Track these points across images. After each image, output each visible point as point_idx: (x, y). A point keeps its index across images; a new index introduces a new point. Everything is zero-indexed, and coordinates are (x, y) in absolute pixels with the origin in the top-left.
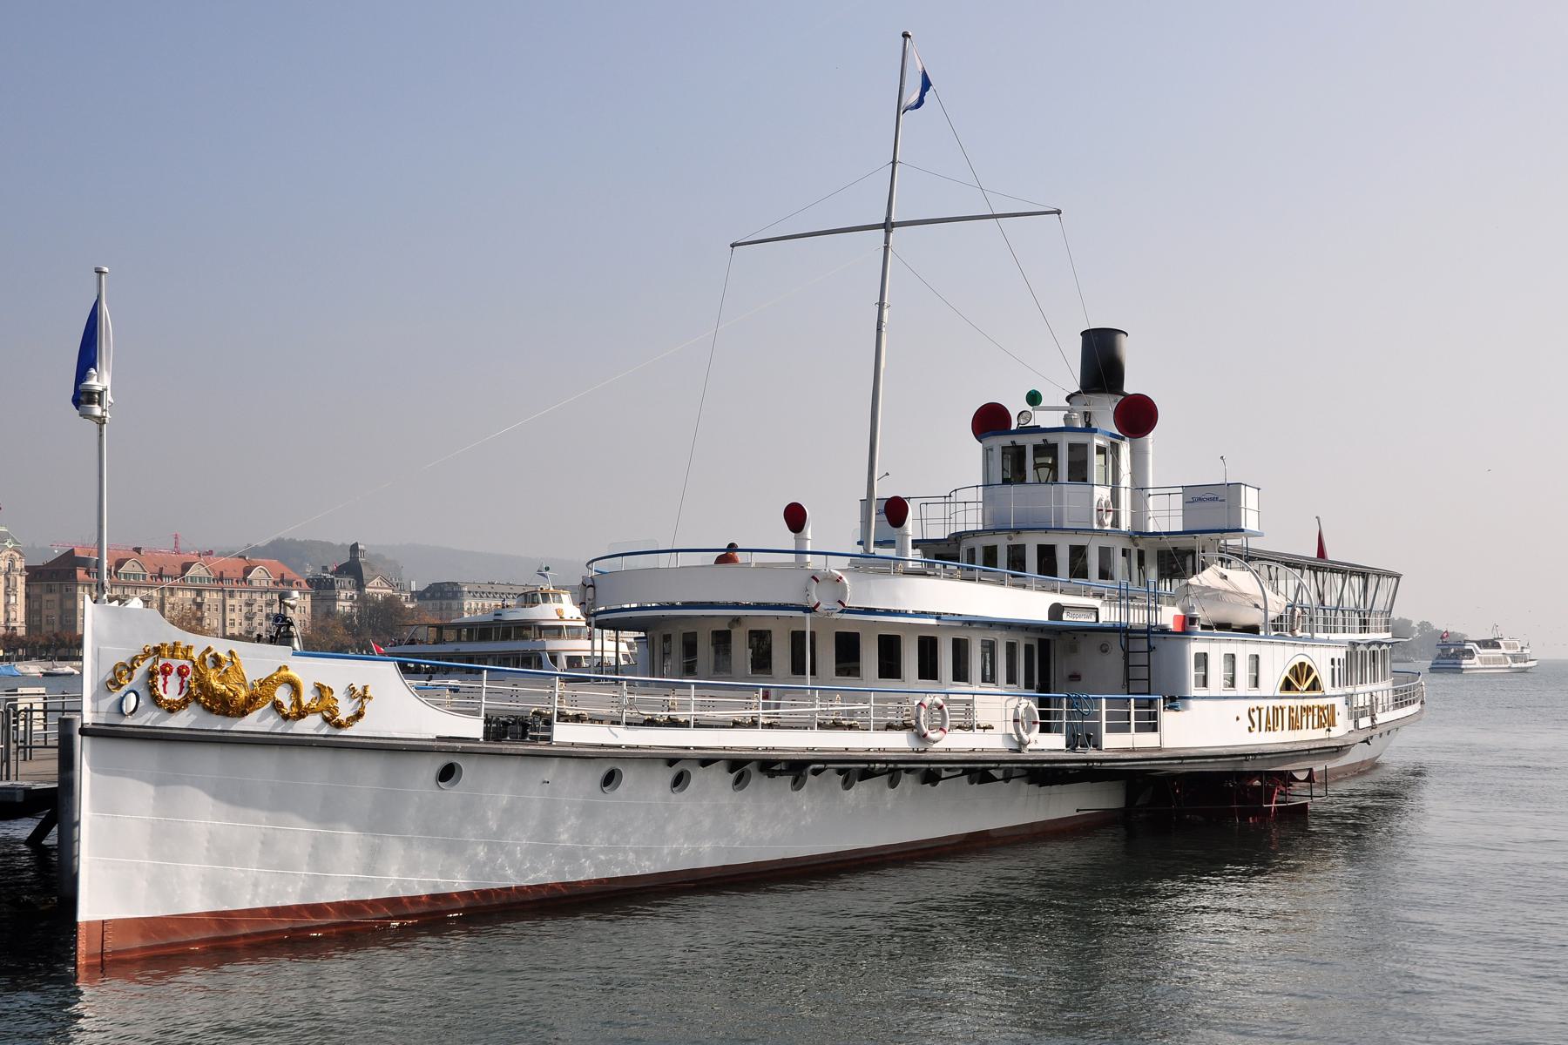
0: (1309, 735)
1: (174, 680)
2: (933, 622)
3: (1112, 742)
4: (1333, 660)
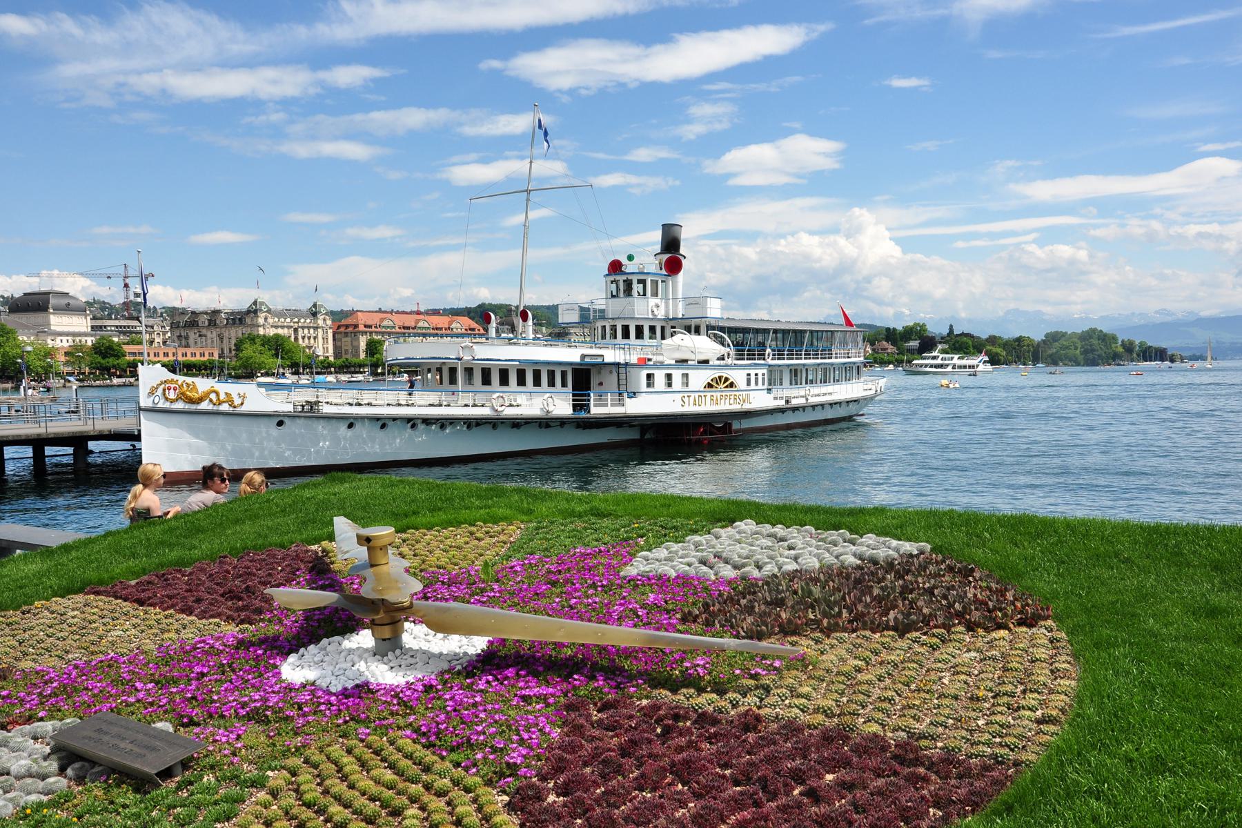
0: (725, 406)
1: (172, 391)
2: (518, 363)
3: (596, 411)
4: (749, 375)
